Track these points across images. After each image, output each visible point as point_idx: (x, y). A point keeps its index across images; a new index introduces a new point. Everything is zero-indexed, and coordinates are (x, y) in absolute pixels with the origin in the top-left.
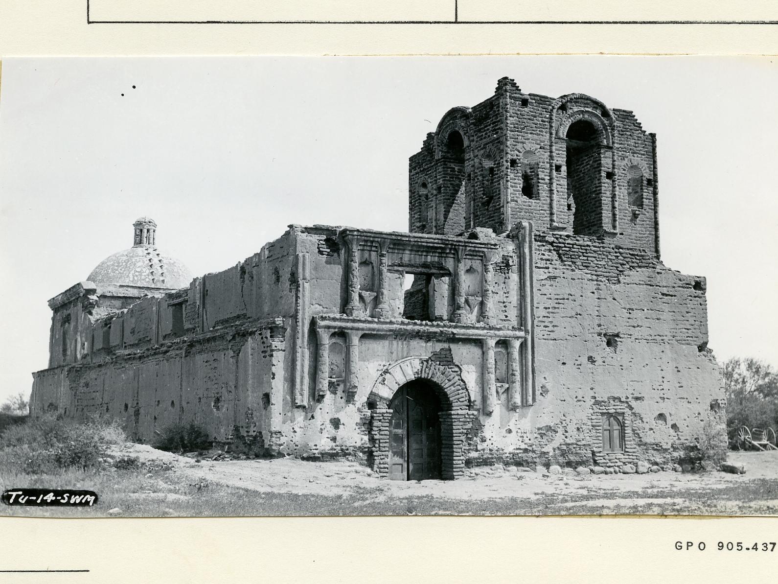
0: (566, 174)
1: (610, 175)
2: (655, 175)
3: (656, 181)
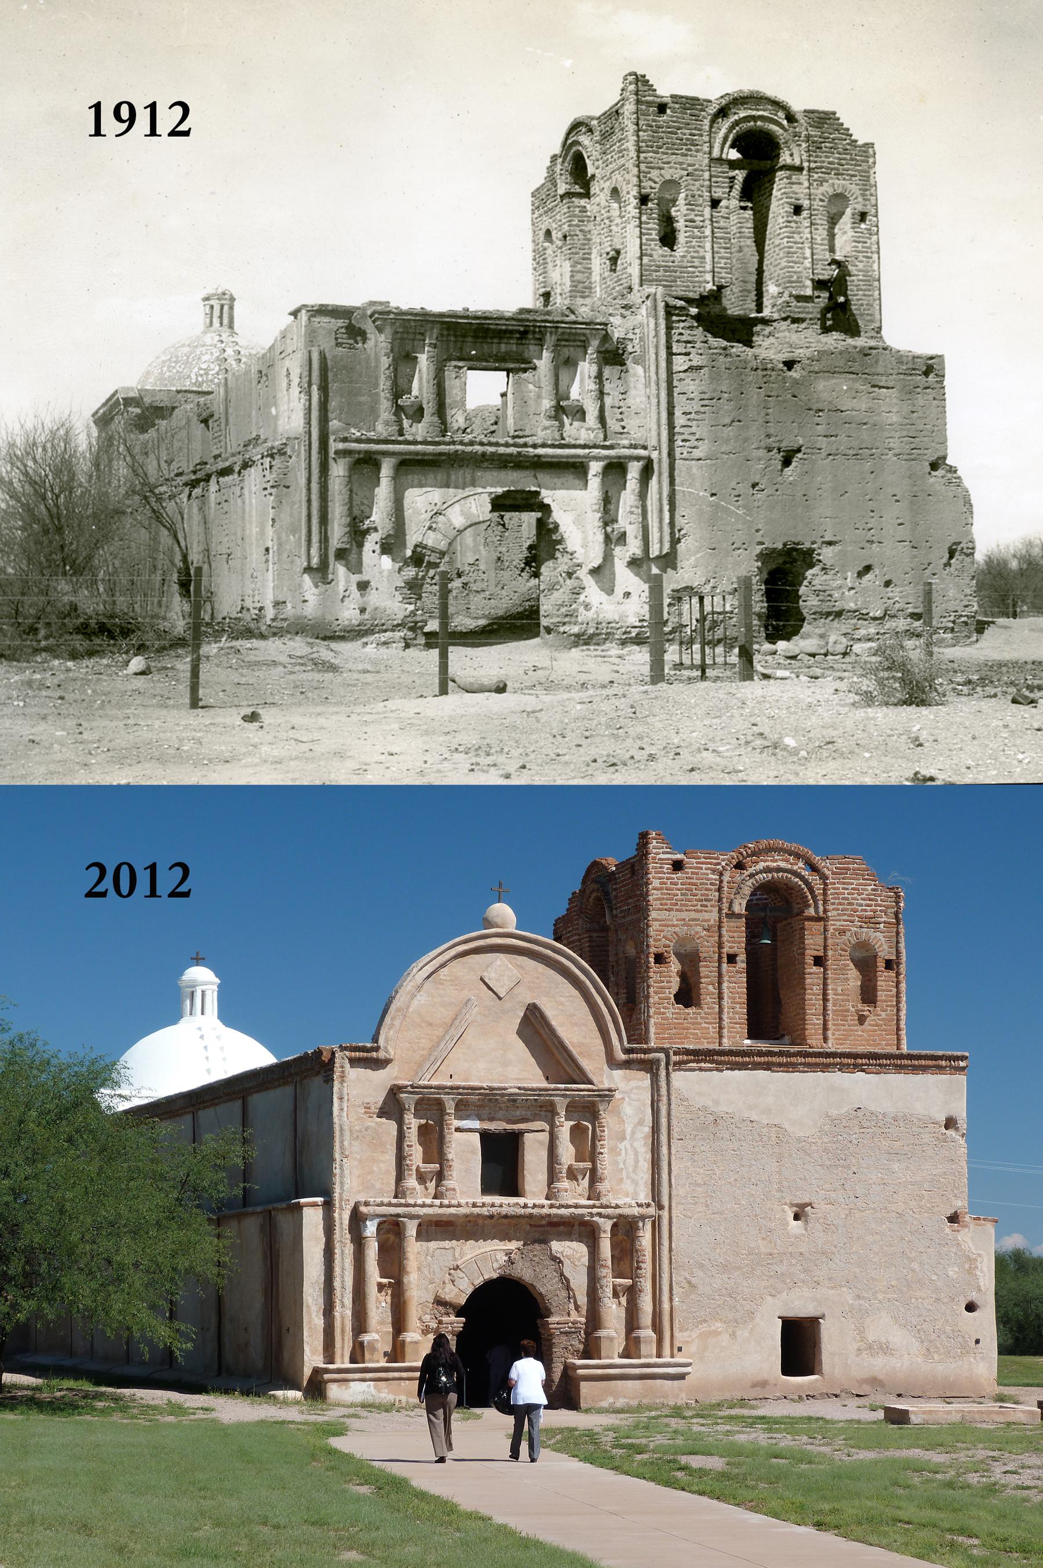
0: (744, 965)
1: (819, 961)
2: (898, 952)
3: (898, 964)
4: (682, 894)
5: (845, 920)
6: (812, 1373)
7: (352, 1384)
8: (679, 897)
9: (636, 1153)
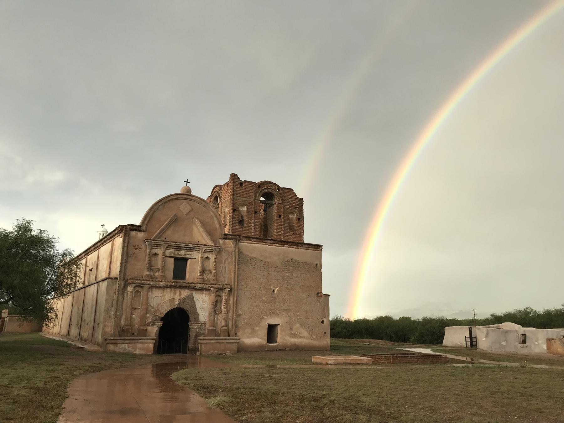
4: (243, 193)
5: (288, 206)
6: (276, 343)
7: (119, 345)
8: (242, 193)
9: (225, 268)
